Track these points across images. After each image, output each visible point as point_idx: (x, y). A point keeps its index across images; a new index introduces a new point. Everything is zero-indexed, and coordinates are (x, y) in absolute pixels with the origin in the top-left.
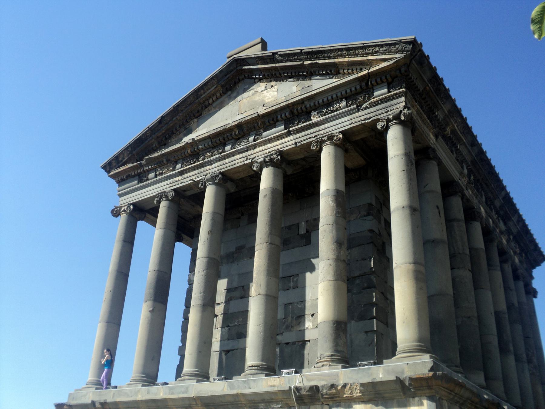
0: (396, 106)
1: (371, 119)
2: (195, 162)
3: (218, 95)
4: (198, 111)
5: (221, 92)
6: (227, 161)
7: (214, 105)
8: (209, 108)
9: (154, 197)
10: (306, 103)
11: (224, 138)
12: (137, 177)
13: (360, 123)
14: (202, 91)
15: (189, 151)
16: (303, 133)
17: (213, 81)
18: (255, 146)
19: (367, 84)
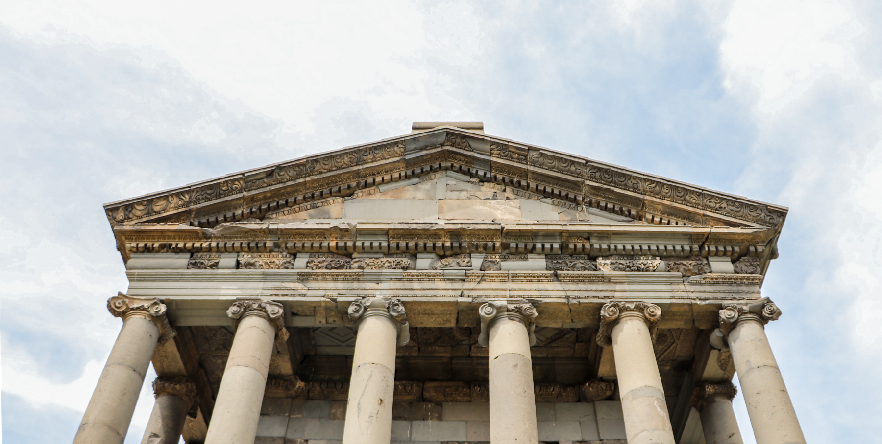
0: (749, 296)
1: (707, 302)
2: (341, 267)
3: (396, 175)
4: (349, 187)
5: (403, 174)
6: (416, 285)
7: (383, 188)
8: (372, 189)
9: (231, 303)
10: (593, 241)
11: (416, 245)
12: (188, 255)
13: (689, 301)
14: (371, 156)
15: (333, 244)
16: (581, 286)
17: (396, 148)
18: (482, 279)
19: (701, 248)
